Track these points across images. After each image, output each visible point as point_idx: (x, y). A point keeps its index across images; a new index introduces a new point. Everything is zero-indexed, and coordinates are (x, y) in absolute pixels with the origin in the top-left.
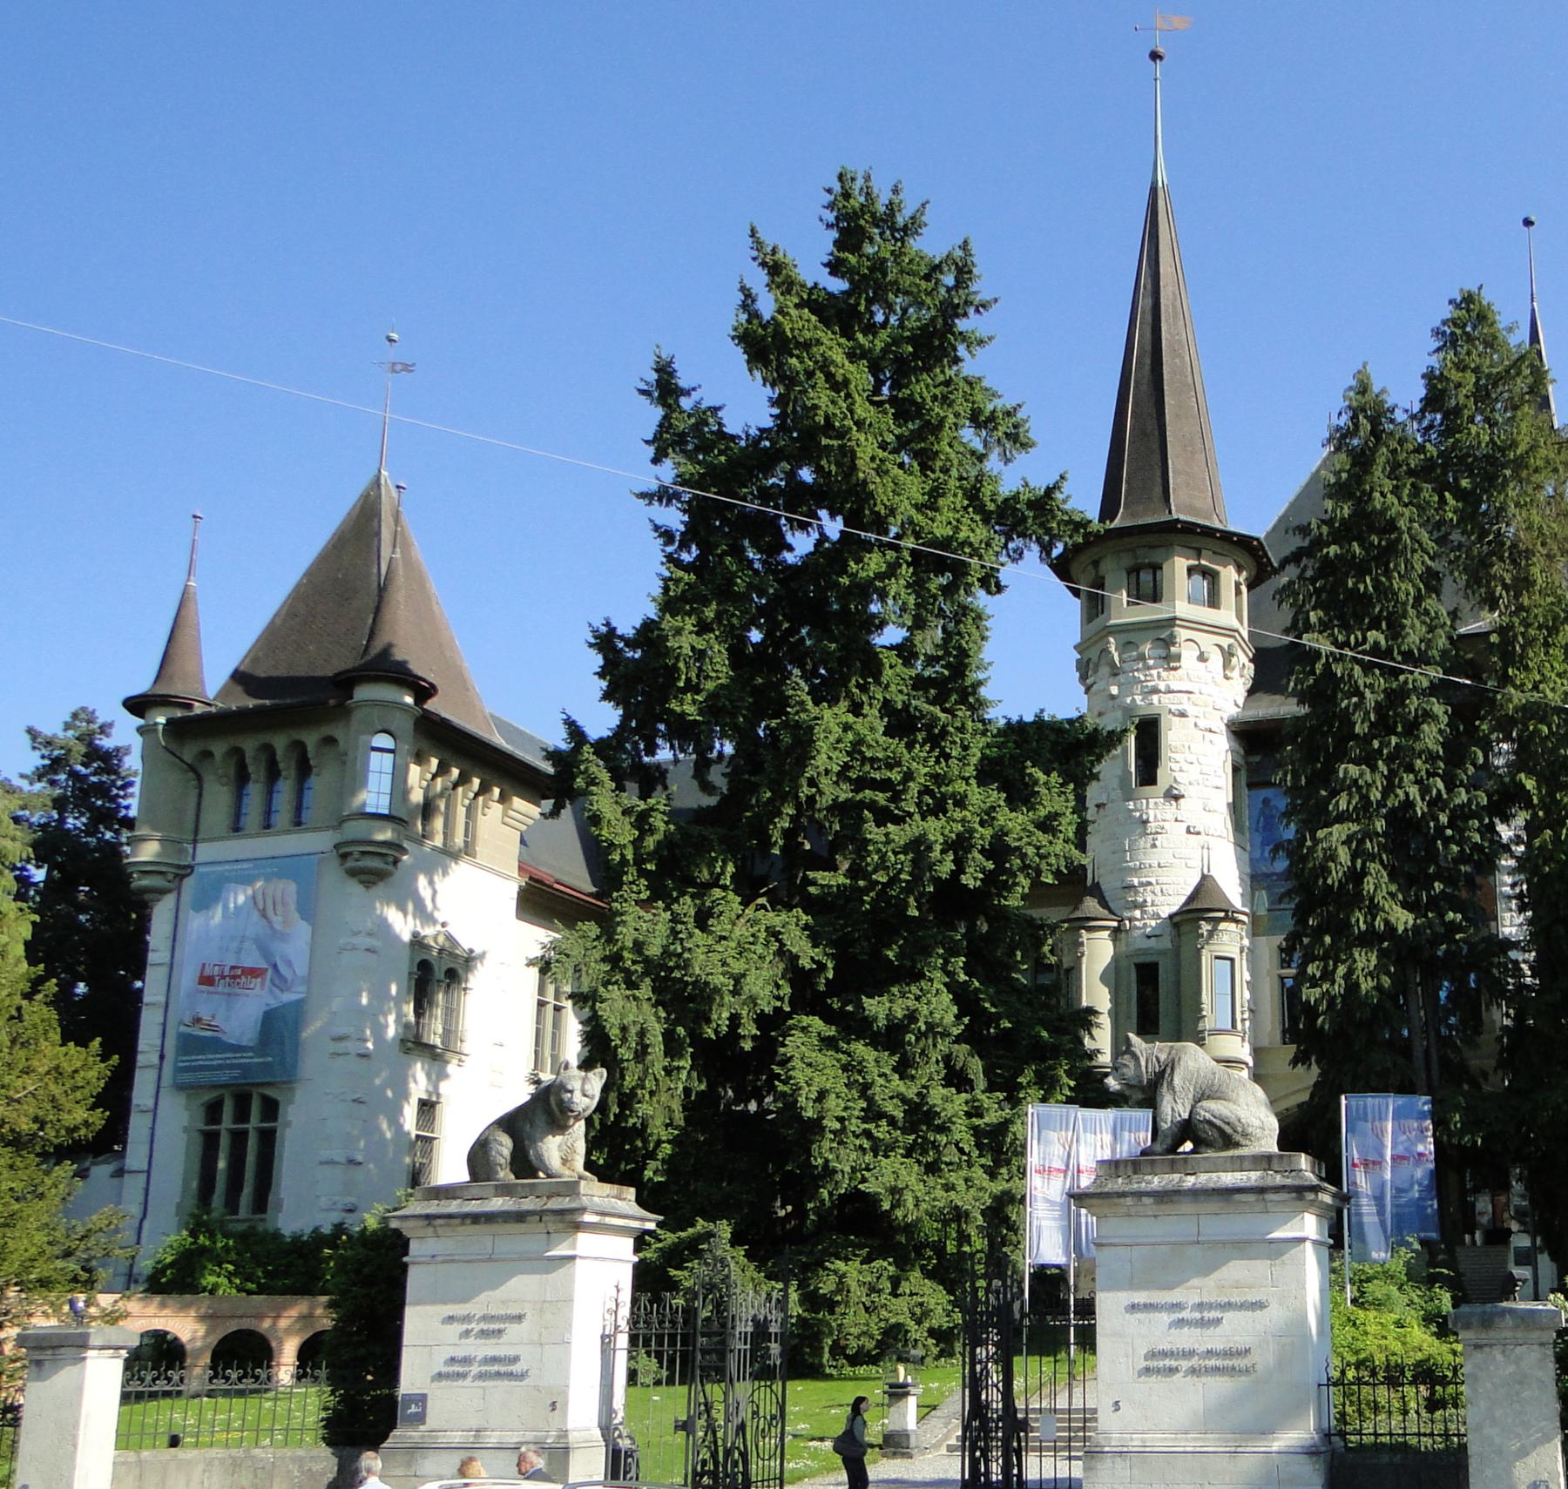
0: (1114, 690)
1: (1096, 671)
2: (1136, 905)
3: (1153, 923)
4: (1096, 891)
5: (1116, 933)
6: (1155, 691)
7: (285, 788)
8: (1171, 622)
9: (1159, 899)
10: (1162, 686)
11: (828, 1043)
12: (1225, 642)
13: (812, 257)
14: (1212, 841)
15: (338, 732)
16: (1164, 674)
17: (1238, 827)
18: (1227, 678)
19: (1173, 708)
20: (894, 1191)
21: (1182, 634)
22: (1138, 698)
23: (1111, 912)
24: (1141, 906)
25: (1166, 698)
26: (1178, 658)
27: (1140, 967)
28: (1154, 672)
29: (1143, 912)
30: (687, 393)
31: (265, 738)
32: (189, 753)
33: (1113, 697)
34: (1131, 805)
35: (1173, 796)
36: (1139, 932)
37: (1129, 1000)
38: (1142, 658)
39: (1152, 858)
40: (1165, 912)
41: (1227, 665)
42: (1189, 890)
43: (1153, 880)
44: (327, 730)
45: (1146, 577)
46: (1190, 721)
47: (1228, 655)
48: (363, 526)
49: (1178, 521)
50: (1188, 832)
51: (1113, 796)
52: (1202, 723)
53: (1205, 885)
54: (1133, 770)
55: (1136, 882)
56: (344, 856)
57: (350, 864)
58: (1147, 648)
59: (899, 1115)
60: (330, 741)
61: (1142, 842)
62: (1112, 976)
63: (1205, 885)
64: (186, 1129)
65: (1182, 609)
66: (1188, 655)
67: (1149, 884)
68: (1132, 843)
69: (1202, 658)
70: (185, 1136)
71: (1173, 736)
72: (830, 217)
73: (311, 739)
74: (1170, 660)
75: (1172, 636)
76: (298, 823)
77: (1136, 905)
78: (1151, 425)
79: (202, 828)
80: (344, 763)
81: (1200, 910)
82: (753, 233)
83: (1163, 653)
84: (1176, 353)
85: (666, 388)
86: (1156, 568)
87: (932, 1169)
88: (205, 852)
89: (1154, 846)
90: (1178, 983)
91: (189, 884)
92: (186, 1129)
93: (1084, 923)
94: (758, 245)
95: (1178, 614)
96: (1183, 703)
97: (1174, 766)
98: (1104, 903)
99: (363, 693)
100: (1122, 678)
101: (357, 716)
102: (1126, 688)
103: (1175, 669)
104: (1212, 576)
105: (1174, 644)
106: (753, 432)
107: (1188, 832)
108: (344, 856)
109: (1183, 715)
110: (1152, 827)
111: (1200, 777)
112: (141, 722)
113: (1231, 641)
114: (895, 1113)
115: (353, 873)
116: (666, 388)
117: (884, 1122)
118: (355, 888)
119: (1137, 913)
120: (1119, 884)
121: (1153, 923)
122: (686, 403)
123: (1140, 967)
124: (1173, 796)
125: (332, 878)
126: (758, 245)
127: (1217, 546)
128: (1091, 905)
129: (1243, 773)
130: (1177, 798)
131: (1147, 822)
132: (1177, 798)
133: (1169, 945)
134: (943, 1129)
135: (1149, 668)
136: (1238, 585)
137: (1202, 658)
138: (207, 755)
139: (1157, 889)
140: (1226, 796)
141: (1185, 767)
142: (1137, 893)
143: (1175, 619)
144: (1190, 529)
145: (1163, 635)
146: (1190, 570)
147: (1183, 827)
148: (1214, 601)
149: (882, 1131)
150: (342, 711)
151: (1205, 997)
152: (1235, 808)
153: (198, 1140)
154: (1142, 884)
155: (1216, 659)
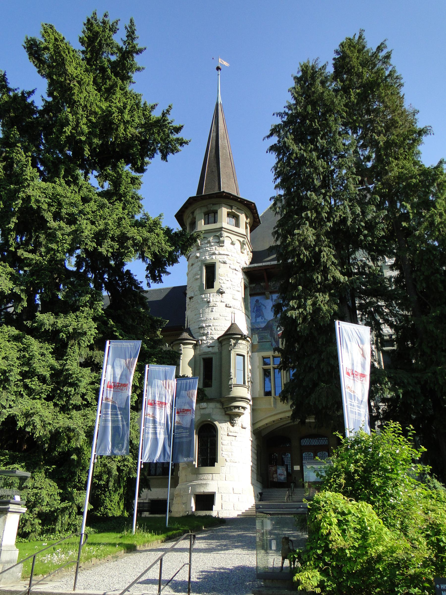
0: (198, 255)
2: (204, 335)
3: (211, 341)
4: (188, 331)
5: (195, 346)
6: (214, 254)
8: (221, 229)
9: (213, 332)
10: (217, 252)
11: (17, 339)
12: (242, 239)
14: (236, 311)
16: (217, 248)
17: (246, 308)
18: (242, 253)
19: (221, 260)
20: (27, 415)
21: (225, 234)
22: (207, 257)
23: (194, 338)
24: (206, 335)
25: (218, 257)
26: (223, 242)
27: (204, 360)
28: (214, 247)
29: (207, 337)
33: (197, 257)
34: (203, 296)
35: (220, 292)
36: (205, 345)
37: (200, 366)
38: (209, 242)
39: (211, 316)
40: (216, 337)
41: (242, 248)
42: (226, 329)
43: (211, 325)
45: (211, 215)
46: (228, 265)
47: (243, 244)
49: (224, 192)
50: (226, 306)
51: (196, 293)
52: (232, 267)
53: (233, 326)
54: (204, 283)
55: (204, 325)
58: (211, 239)
59: (48, 375)
61: (207, 310)
62: (193, 363)
63: (233, 326)
65: (225, 225)
66: (227, 242)
67: (210, 326)
68: (203, 310)
69: (233, 243)
71: (220, 270)
74: (220, 243)
75: (221, 234)
77: (204, 335)
78: (215, 169)
83: (217, 241)
86: (215, 212)
87: (64, 409)
89: (212, 311)
90: (221, 366)
93: (183, 342)
95: (223, 226)
96: (225, 258)
97: (221, 281)
98: (191, 335)
100: (201, 250)
102: (203, 254)
103: (222, 246)
104: (236, 217)
105: (222, 237)
107: (226, 306)
109: (225, 263)
110: (211, 304)
111: (231, 286)
113: (244, 239)
114: (44, 373)
117: (36, 379)
119: (204, 338)
120: (197, 327)
121: (211, 341)
123: (204, 360)
124: (220, 292)
127: (239, 205)
128: (185, 335)
129: (248, 289)
130: (222, 293)
131: (209, 302)
132: (222, 293)
133: (217, 351)
134: (74, 385)
135: (212, 246)
136: (246, 223)
137: (233, 243)
139: (213, 328)
140: (241, 295)
141: (225, 282)
142: (204, 330)
143: (222, 228)
145: (218, 234)
146: (229, 214)
147: (224, 304)
149: (34, 384)
151: (232, 370)
152: (245, 300)
154: (207, 326)
155: (238, 245)
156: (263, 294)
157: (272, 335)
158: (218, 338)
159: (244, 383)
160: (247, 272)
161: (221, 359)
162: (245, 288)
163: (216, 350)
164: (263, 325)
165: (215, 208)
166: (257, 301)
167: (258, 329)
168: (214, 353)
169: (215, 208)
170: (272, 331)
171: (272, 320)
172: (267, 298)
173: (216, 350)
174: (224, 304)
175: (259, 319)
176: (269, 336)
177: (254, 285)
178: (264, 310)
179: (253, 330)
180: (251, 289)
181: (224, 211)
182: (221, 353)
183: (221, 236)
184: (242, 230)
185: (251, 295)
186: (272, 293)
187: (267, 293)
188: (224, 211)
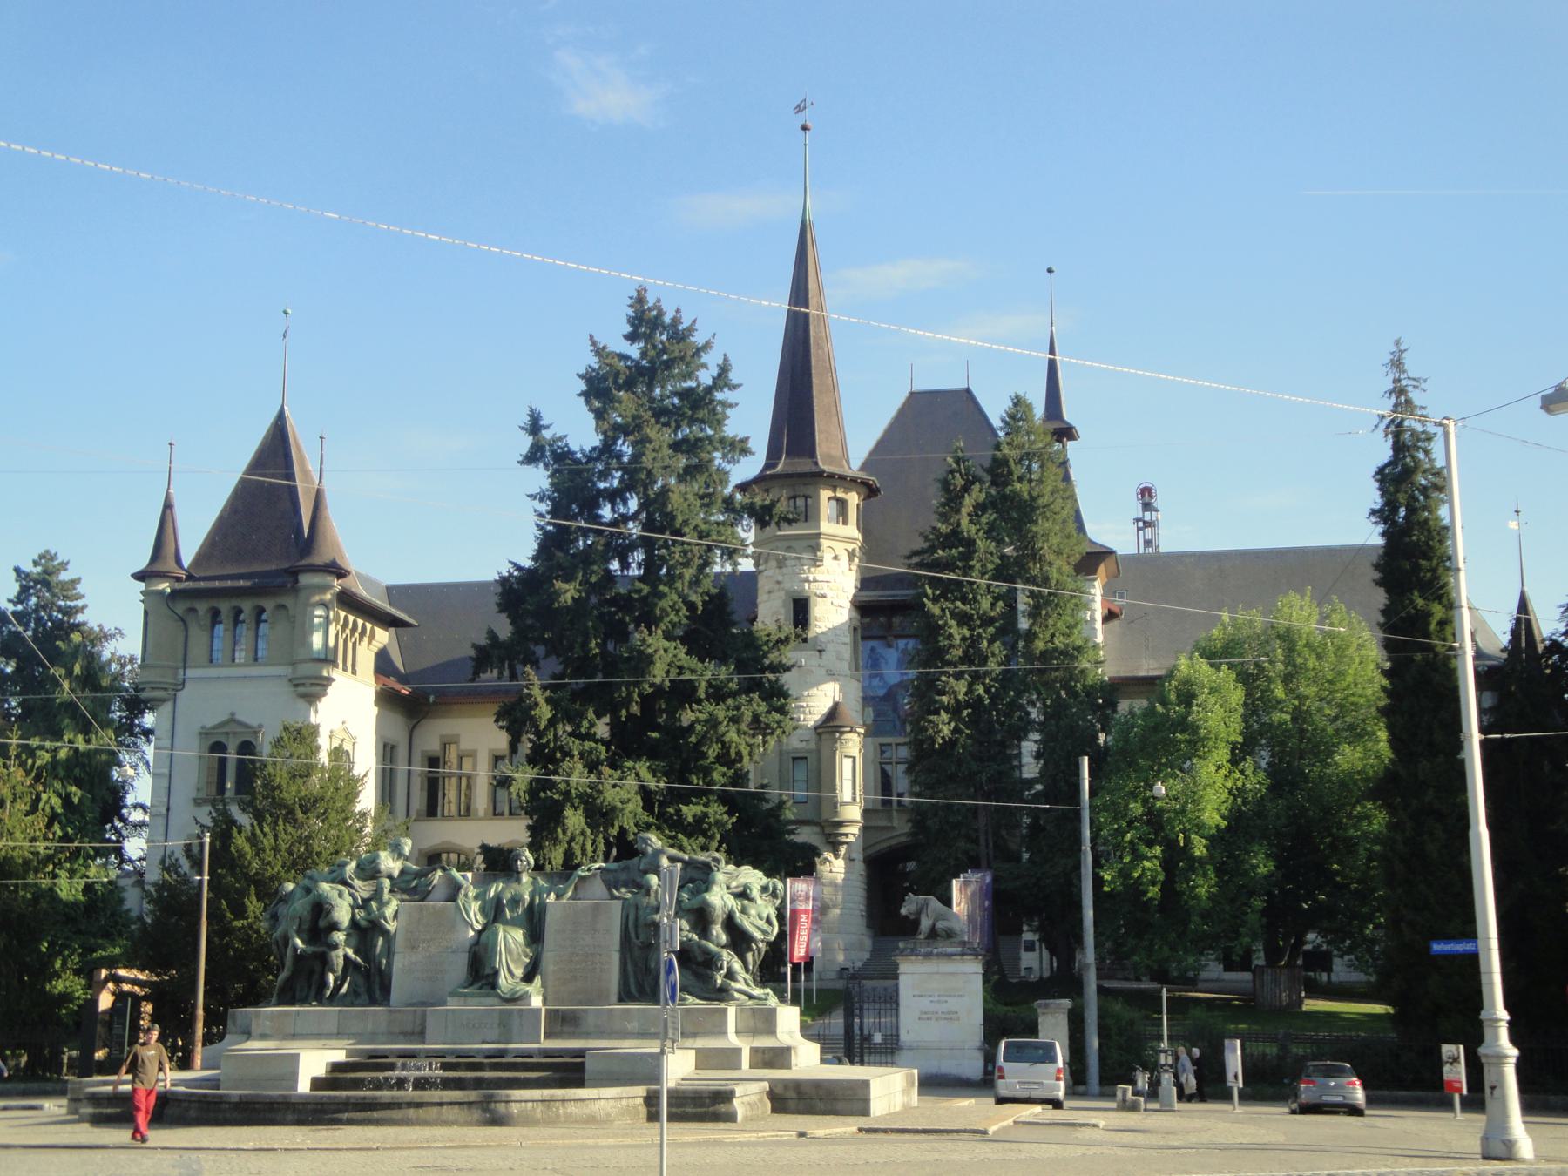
1: (766, 561)
7: (245, 632)
15: (287, 601)
21: (824, 543)
30: (547, 427)
31: (235, 602)
32: (180, 607)
40: (811, 724)
41: (851, 560)
46: (827, 601)
47: (851, 555)
48: (277, 449)
63: (836, 705)
69: (836, 558)
72: (631, 313)
73: (269, 604)
74: (816, 562)
76: (256, 660)
79: (190, 655)
81: (831, 724)
82: (591, 337)
84: (819, 347)
85: (535, 426)
88: (190, 673)
91: (181, 695)
94: (594, 343)
106: (587, 449)
108: (296, 685)
109: (823, 596)
112: (142, 586)
116: (535, 426)
118: (301, 704)
122: (547, 434)
126: (594, 343)
137: (836, 558)
138: (193, 610)
144: (831, 476)
148: (845, 522)
150: (295, 590)
155: (844, 557)
157: (895, 710)
158: (816, 728)
159: (854, 799)
161: (819, 760)
163: (812, 745)
164: (881, 693)
165: (809, 490)
166: (873, 649)
167: (873, 698)
172: (890, 646)
173: (812, 745)
175: (876, 682)
179: (867, 700)
180: (864, 627)
181: (825, 494)
182: (819, 751)
183: (815, 548)
184: (852, 530)
185: (863, 638)
186: (898, 637)
188: (825, 494)
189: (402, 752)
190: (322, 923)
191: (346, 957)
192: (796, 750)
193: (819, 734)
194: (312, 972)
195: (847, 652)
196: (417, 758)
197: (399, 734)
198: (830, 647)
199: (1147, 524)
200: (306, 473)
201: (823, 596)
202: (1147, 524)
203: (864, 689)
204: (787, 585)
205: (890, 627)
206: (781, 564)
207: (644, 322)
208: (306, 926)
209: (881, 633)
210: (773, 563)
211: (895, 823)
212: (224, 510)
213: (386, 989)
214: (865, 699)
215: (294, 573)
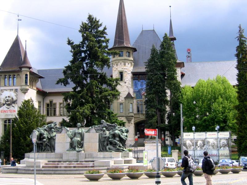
1: (114, 65)
12: (131, 62)
13: (86, 21)
31: (9, 74)
44: (18, 73)
53: (129, 94)
56: (22, 90)
57: (23, 91)
60: (19, 75)
63: (129, 94)
64: (2, 124)
70: (2, 125)
73: (16, 74)
80: (21, 78)
92: (2, 124)
99: (23, 69)
101: (23, 72)
108: (22, 90)
115: (23, 92)
118: (23, 94)
125: (19, 92)
153: (4, 126)
155: (130, 64)
156: (138, 80)
160: (132, 73)
162: (132, 78)
163: (124, 101)
164: (137, 90)
166: (135, 82)
168: (123, 102)
169: (122, 51)
170: (140, 93)
171: (140, 89)
172: (139, 81)
173: (124, 101)
174: (126, 86)
175: (136, 88)
176: (139, 94)
177: (134, 76)
178: (138, 86)
180: (133, 77)
185: (133, 80)
186: (140, 79)
187: (139, 80)
189: (42, 103)
190: (42, 137)
191: (46, 143)
192: (121, 102)
193: (125, 99)
194: (40, 147)
195: (130, 83)
196: (45, 104)
197: (41, 100)
198: (127, 82)
199: (189, 57)
200: (23, 48)
201: (126, 72)
202: (189, 57)
203: (134, 90)
204: (118, 69)
205: (139, 77)
206: (117, 65)
207: (90, 18)
208: (39, 138)
209: (137, 79)
210: (116, 65)
211: (140, 116)
212: (6, 55)
213: (54, 149)
214: (134, 92)
215: (21, 68)
